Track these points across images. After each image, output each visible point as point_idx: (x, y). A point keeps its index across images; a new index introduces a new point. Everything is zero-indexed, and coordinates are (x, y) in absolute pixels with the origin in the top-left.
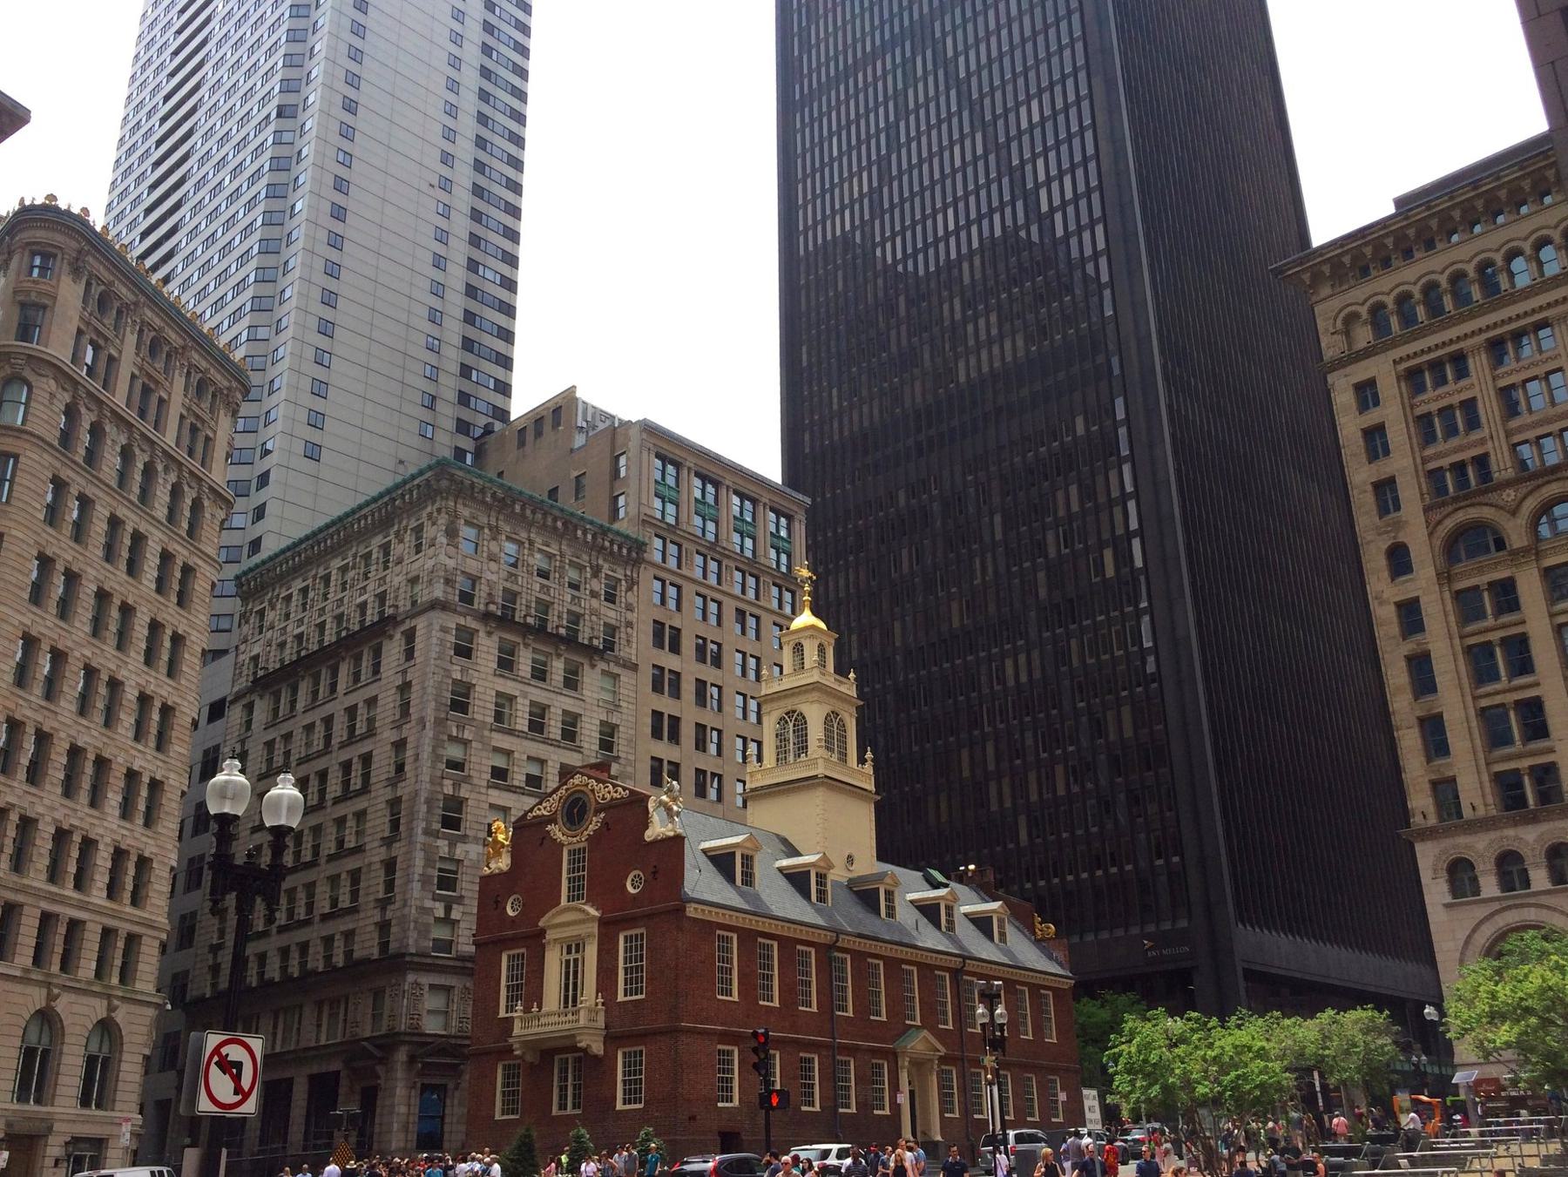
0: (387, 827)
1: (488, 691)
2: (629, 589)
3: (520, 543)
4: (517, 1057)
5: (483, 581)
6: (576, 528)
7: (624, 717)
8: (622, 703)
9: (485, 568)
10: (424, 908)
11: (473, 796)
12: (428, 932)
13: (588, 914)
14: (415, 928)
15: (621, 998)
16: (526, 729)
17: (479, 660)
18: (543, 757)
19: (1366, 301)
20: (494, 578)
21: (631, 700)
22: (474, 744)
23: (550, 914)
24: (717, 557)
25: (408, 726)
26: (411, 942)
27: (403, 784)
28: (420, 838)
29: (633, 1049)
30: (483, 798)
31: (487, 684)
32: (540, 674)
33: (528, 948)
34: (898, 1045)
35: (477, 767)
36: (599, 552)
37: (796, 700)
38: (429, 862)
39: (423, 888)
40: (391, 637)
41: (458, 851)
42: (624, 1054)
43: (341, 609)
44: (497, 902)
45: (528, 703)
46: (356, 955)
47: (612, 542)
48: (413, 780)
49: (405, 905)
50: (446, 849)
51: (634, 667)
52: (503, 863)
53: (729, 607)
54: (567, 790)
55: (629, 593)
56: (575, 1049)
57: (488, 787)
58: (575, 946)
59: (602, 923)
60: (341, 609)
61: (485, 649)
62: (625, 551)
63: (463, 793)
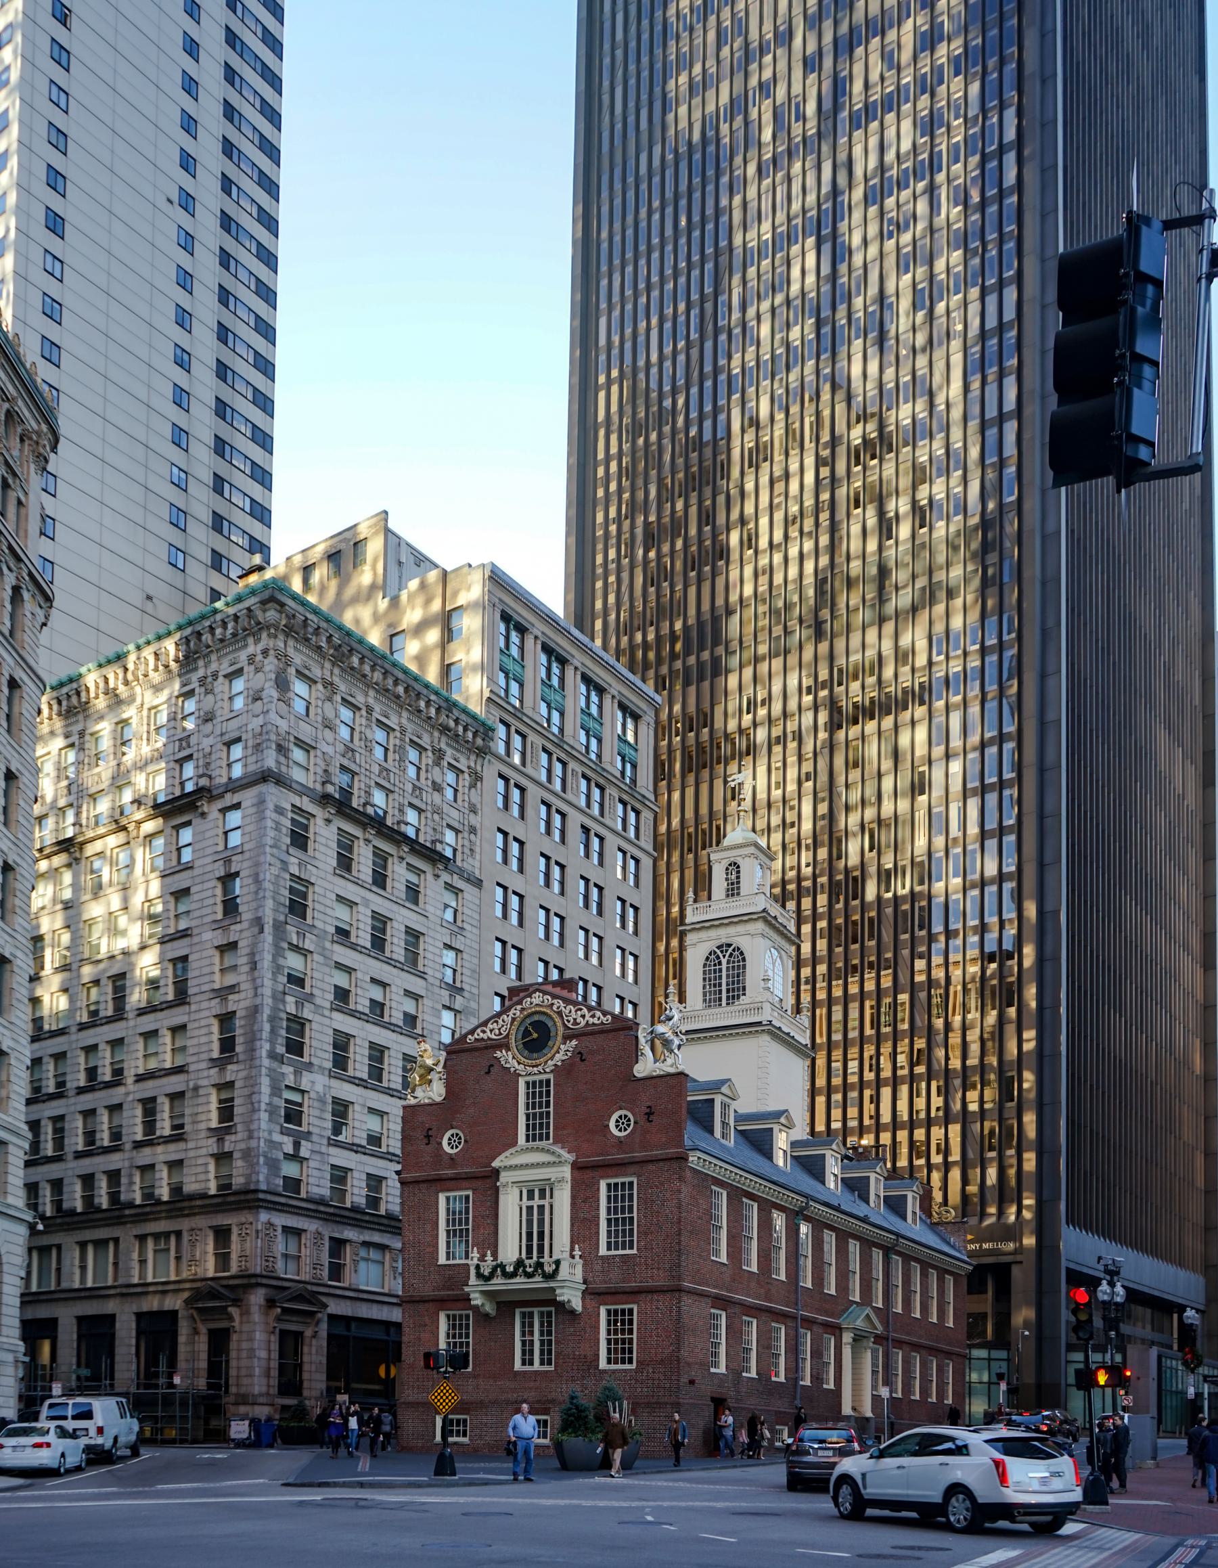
0: (216, 1047)
1: (329, 894)
2: (473, 786)
4: (476, 1309)
7: (468, 943)
8: (466, 926)
11: (317, 1018)
12: (279, 1169)
13: (559, 1156)
14: (266, 1163)
15: (603, 1251)
16: (368, 945)
21: (475, 923)
22: (316, 957)
23: (507, 1153)
24: (563, 756)
25: (238, 927)
26: (261, 1178)
28: (266, 1062)
29: (619, 1307)
30: (327, 1021)
32: (380, 880)
33: (474, 1190)
34: (843, 1322)
35: (319, 984)
37: (731, 930)
39: (270, 1120)
42: (609, 1312)
44: (428, 1137)
45: (370, 914)
48: (250, 993)
49: (250, 1137)
51: (478, 883)
52: (436, 1091)
53: (575, 819)
54: (523, 1009)
56: (553, 1302)
57: (332, 1009)
58: (546, 1190)
59: (576, 1167)
63: (307, 1014)
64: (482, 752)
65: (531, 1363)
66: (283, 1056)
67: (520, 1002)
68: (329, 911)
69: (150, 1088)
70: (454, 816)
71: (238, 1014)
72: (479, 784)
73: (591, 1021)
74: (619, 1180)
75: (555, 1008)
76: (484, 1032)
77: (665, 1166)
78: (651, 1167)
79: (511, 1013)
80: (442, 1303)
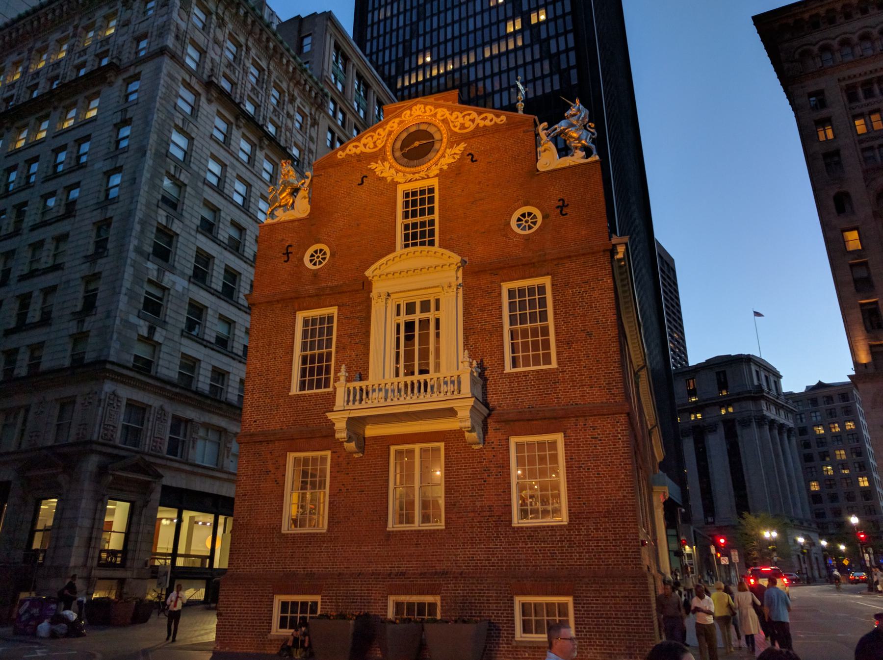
1: (204, 149)
2: (313, 125)
3: (238, 45)
5: (208, 55)
6: (282, 55)
9: (210, 45)
10: (127, 321)
15: (508, 368)
17: (199, 119)
18: (244, 225)
19: (817, 43)
20: (217, 58)
22: (188, 189)
27: (114, 206)
30: (193, 239)
31: (204, 143)
35: (189, 210)
38: (138, 279)
40: (111, 84)
41: (166, 279)
43: (56, 72)
46: (45, 365)
47: (306, 81)
49: (108, 317)
50: (155, 273)
54: (401, 122)
55: (312, 129)
57: (197, 231)
60: (56, 72)
61: (205, 113)
62: (313, 94)
63: (176, 227)
64: (321, 107)
65: (410, 520)
66: (149, 255)
68: (203, 161)
69: (25, 287)
71: (115, 219)
72: (316, 127)
75: (439, 116)
76: (356, 147)
79: (388, 128)
80: (294, 442)
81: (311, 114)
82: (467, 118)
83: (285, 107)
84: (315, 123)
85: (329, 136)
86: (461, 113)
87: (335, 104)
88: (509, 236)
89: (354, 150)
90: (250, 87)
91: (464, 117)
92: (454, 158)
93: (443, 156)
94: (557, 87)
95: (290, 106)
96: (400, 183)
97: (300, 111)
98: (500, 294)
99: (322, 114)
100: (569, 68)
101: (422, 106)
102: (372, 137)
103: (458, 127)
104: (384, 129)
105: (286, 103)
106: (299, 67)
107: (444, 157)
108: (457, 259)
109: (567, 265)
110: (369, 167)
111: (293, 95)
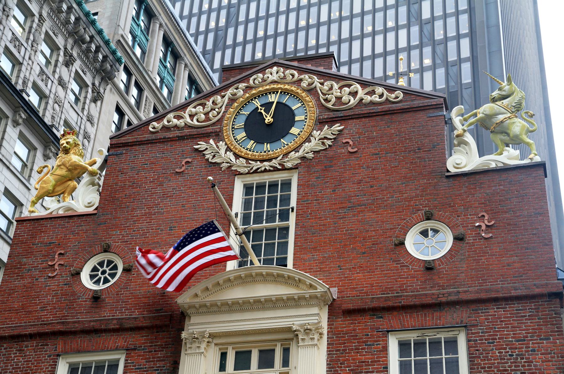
2: (95, 100)
36: (75, 42)
47: (92, 37)
67: (245, 79)
70: (73, 118)
72: (99, 103)
73: (368, 98)
74: (429, 336)
75: (304, 84)
76: (179, 117)
77: (527, 309)
78: (493, 310)
81: (93, 84)
82: (346, 89)
83: (58, 70)
84: (97, 98)
85: (116, 117)
86: (337, 83)
87: (129, 74)
88: (402, 260)
89: (175, 121)
90: (10, 36)
91: (341, 88)
92: (323, 144)
93: (308, 140)
94: (441, 85)
95: (64, 69)
96: (241, 174)
97: (79, 79)
98: (385, 349)
99: (109, 86)
100: (460, 61)
101: (282, 69)
102: (204, 105)
103: (332, 103)
104: (223, 97)
105: (59, 65)
106: (84, 18)
107: (310, 141)
108: (321, 288)
109: (491, 312)
110: (195, 147)
111: (71, 56)
